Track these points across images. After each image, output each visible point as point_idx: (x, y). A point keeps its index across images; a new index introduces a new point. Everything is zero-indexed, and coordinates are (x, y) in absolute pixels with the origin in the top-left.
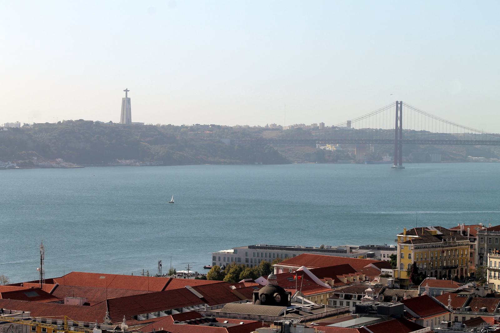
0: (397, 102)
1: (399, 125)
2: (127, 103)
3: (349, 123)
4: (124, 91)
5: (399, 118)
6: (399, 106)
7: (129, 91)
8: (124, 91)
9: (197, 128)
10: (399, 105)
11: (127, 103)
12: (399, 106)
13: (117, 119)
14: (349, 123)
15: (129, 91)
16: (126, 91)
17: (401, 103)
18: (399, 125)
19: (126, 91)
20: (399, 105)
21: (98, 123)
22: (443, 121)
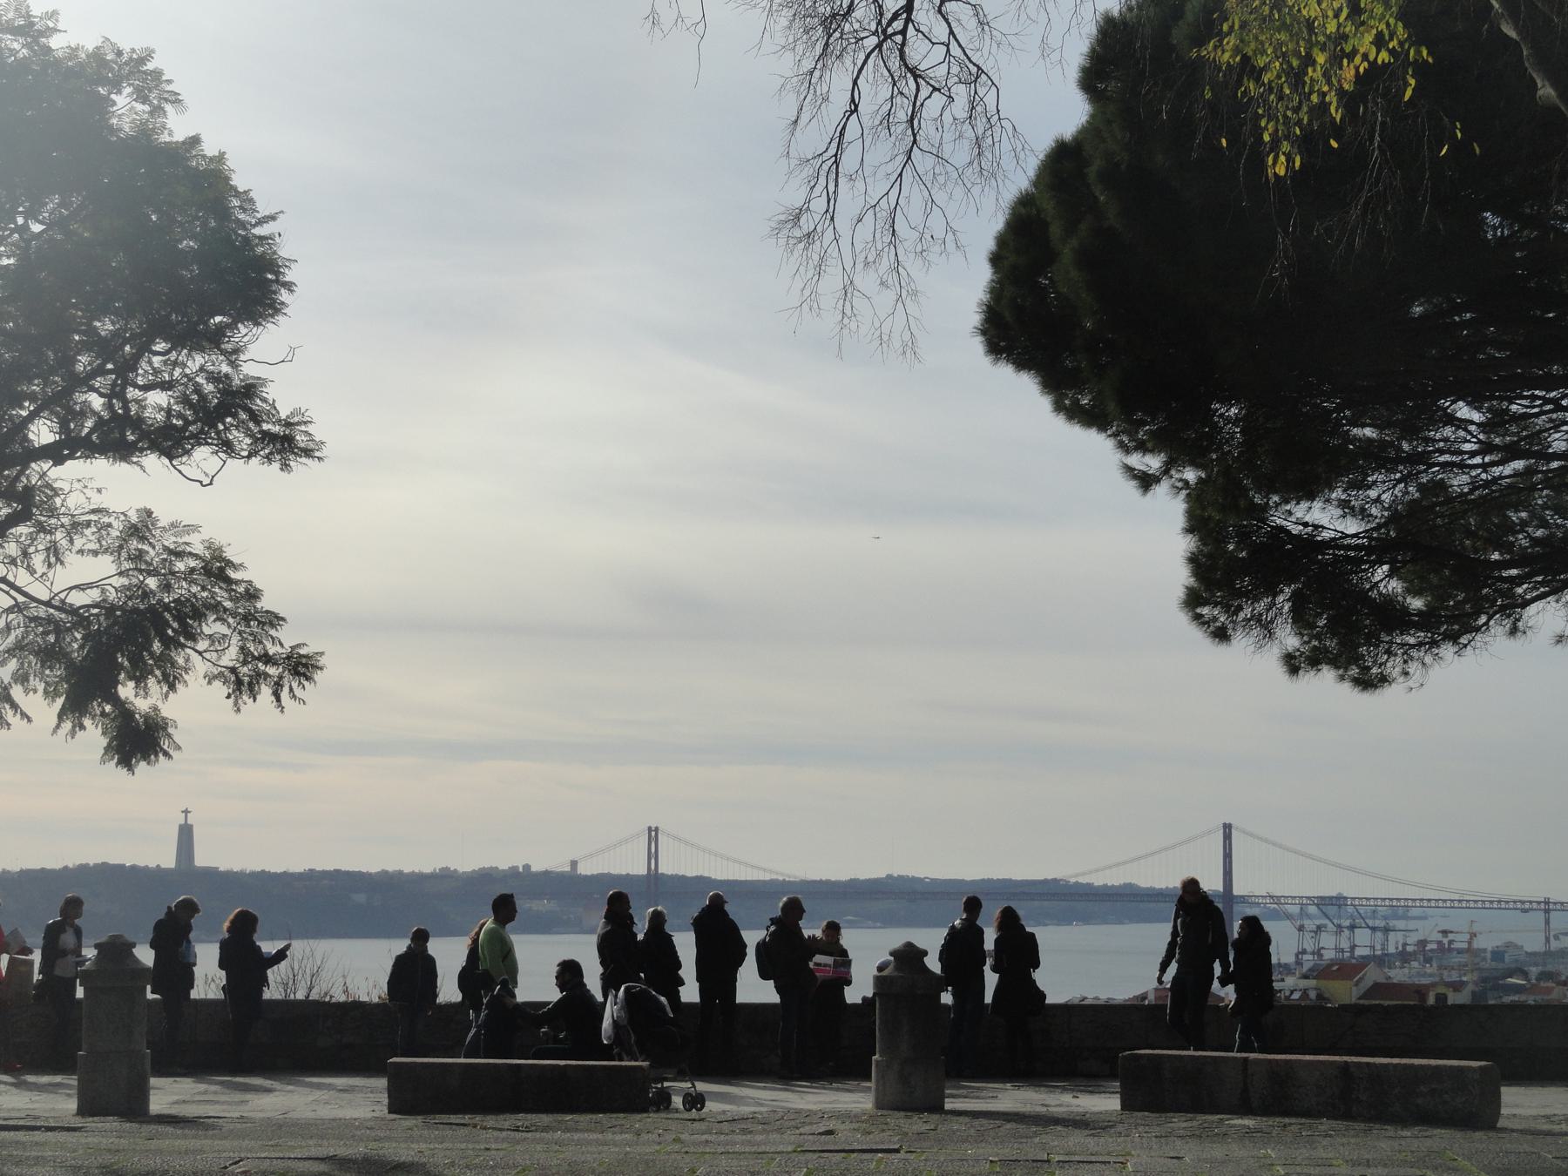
0: (650, 829)
1: (653, 867)
2: (186, 833)
3: (574, 864)
4: (183, 812)
5: (653, 856)
6: (653, 834)
7: (189, 812)
8: (183, 812)
9: (311, 875)
10: (653, 834)
11: (186, 833)
12: (653, 834)
13: (168, 860)
14: (574, 864)
15: (189, 812)
16: (186, 812)
17: (657, 829)
18: (653, 867)
19: (186, 812)
20: (653, 834)
21: (133, 867)
22: (728, 859)
